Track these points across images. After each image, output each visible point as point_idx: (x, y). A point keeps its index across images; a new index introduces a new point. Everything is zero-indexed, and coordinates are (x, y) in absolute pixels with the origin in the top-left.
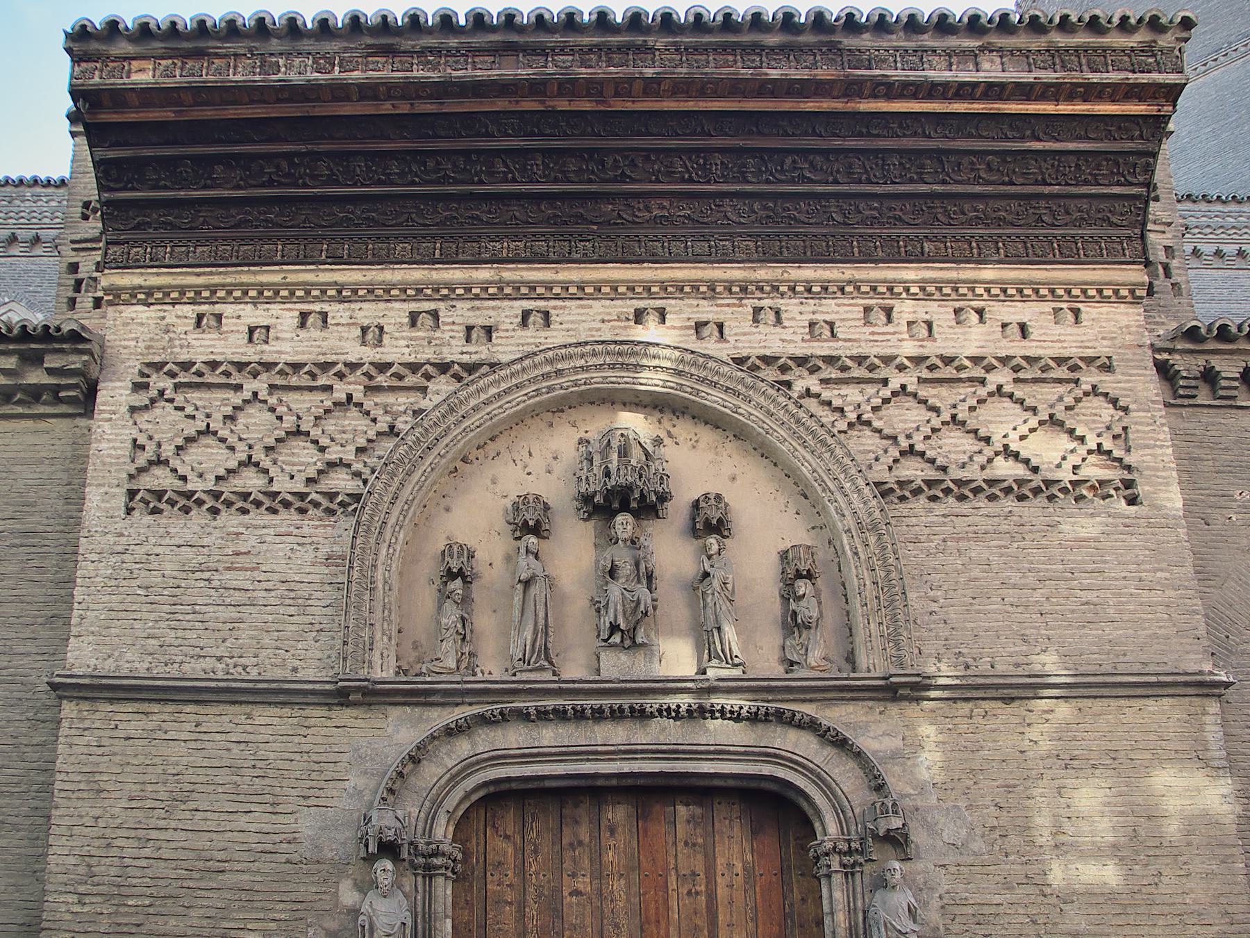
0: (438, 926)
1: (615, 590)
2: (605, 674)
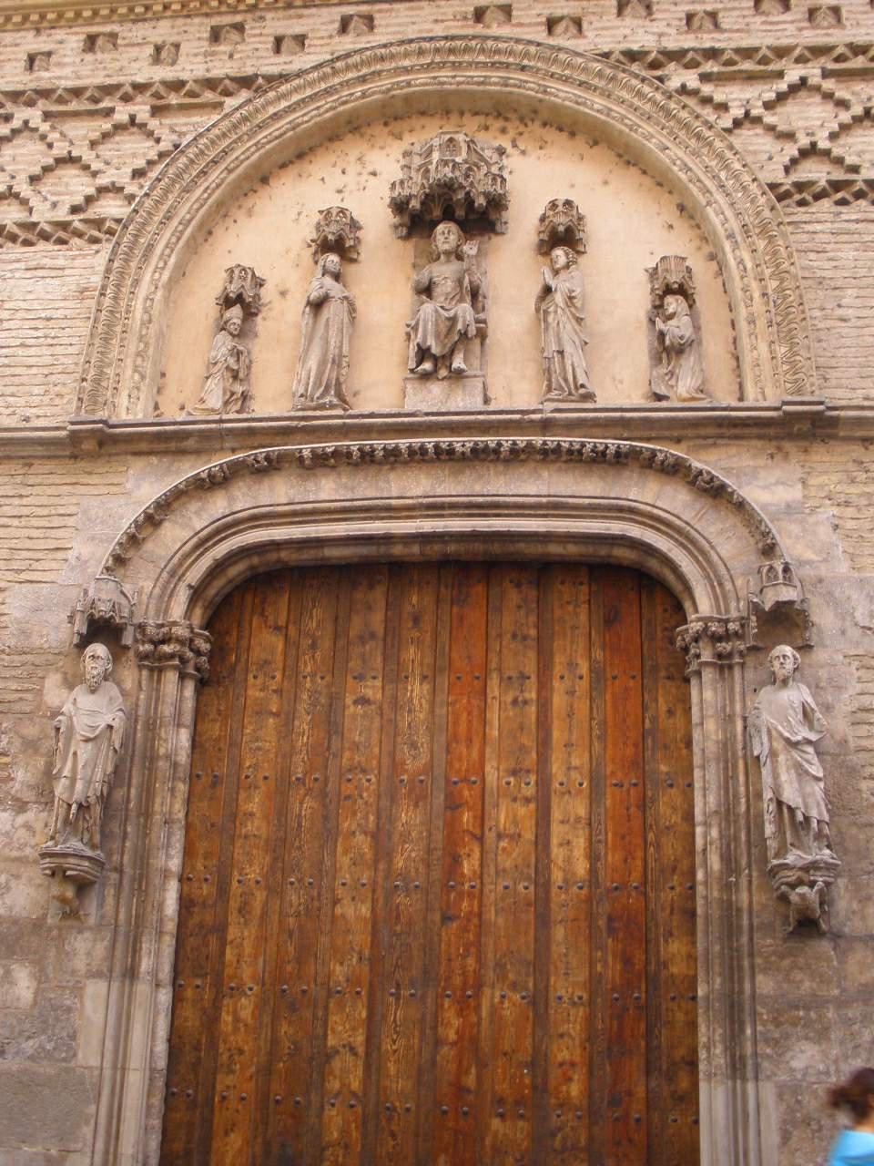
0: (163, 735)
1: (428, 308)
2: (408, 408)
